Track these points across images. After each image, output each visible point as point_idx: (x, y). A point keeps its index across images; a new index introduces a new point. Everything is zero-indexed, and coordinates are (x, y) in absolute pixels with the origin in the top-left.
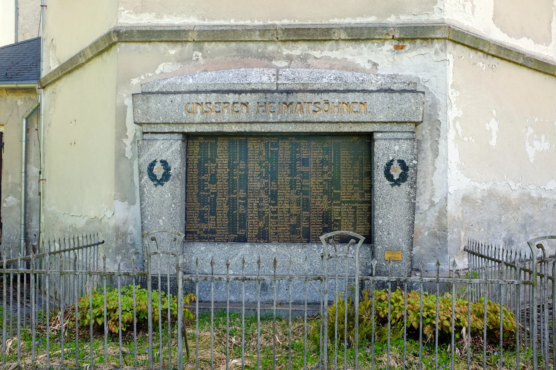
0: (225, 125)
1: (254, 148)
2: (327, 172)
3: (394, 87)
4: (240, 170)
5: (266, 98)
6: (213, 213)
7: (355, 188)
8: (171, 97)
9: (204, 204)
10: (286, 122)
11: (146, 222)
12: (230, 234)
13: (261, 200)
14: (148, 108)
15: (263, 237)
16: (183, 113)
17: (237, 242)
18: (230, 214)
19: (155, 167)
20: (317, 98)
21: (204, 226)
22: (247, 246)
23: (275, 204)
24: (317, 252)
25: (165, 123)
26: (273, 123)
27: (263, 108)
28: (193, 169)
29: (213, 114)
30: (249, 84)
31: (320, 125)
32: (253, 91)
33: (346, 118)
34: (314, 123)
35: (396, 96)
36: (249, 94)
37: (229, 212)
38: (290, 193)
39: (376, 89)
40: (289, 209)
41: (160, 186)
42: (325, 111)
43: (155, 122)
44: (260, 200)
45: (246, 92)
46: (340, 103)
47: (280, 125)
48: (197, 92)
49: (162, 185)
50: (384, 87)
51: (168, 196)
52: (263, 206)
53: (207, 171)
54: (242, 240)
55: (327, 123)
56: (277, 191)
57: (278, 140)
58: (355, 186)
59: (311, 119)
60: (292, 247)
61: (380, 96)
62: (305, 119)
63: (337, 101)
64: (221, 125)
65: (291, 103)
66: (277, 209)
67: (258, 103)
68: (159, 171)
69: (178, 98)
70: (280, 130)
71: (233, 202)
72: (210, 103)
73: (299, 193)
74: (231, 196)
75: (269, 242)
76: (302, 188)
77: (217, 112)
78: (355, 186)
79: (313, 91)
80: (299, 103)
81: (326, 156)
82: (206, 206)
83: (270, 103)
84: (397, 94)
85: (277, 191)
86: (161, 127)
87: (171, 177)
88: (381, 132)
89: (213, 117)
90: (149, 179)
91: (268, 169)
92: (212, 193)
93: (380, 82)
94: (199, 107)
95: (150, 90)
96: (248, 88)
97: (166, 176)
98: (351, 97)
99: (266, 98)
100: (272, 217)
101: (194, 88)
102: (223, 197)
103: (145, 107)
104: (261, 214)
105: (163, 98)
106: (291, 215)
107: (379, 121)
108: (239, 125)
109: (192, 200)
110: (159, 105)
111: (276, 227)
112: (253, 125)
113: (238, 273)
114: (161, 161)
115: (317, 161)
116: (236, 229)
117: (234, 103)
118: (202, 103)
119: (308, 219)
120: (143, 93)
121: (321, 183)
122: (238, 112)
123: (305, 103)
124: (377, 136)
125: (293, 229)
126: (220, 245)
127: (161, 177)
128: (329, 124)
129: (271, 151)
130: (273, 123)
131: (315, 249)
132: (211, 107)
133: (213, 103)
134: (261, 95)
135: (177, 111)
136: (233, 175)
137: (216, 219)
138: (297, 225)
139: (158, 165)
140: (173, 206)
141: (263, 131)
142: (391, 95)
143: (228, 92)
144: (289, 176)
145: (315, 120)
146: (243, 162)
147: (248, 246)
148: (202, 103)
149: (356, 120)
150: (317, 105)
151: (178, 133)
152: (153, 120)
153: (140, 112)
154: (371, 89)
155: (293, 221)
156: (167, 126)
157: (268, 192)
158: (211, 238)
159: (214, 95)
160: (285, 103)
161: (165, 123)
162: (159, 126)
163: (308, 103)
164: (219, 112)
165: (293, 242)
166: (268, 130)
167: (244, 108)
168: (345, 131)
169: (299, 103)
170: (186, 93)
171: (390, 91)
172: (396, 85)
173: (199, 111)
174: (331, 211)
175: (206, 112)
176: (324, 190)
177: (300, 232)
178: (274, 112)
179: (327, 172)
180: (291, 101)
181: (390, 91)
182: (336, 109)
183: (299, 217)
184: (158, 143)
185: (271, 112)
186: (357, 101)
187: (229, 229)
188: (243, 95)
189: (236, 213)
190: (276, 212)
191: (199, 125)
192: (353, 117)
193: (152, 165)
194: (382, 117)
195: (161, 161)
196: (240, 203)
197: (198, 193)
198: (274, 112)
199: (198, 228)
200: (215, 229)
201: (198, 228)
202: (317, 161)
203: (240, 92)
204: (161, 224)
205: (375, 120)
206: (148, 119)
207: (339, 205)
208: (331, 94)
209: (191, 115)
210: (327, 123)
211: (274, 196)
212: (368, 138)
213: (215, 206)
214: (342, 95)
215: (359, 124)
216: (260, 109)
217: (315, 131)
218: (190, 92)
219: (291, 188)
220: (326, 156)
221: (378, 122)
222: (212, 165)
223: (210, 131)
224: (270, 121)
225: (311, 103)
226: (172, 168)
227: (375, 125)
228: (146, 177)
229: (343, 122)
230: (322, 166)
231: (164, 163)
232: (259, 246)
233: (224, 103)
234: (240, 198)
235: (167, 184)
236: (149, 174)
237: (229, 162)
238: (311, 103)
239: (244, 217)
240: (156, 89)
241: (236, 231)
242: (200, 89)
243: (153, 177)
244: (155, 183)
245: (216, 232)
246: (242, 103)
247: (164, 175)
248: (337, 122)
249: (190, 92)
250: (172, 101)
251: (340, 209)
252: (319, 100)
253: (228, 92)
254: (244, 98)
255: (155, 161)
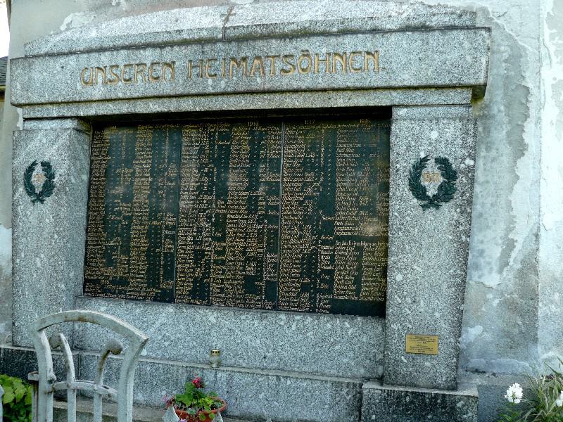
0: (139, 102)
1: (191, 141)
2: (311, 183)
3: (434, 22)
4: (169, 179)
5: (203, 52)
6: (126, 251)
7: (362, 213)
8: (62, 60)
9: (112, 235)
10: (235, 93)
11: (18, 261)
12: (148, 287)
13: (200, 230)
14: (30, 79)
15: (200, 295)
16: (78, 84)
17: (160, 301)
18: (151, 254)
19: (34, 173)
20: (289, 47)
21: (110, 272)
22: (170, 309)
23: (223, 239)
24: (285, 328)
25: (52, 103)
26: (214, 95)
27: (198, 70)
28: (99, 177)
29: (120, 83)
30: (179, 32)
31: (294, 96)
32: (185, 43)
33: (340, 81)
34: (282, 92)
35: (433, 38)
36: (176, 48)
37: (149, 250)
38: (247, 219)
39: (398, 26)
40: (245, 248)
41: (38, 204)
42: (303, 70)
43: (39, 101)
44: (197, 232)
45: (171, 44)
46: (329, 54)
47: (225, 98)
48: (101, 50)
49: (42, 201)
50: (413, 23)
51: (49, 220)
52: (201, 242)
53: (120, 181)
54: (165, 298)
55: (305, 91)
56: (225, 215)
57: (230, 128)
58: (361, 208)
59: (276, 85)
60: (243, 317)
61: (404, 40)
62: (267, 86)
63: (324, 50)
64: (132, 102)
65: (244, 59)
66: (224, 247)
67: (191, 61)
68: (38, 179)
69: (72, 60)
70: (225, 107)
71: (156, 234)
72: (117, 66)
73: (263, 219)
74: (155, 223)
75: (209, 304)
76: (267, 212)
77: (125, 80)
78: (361, 208)
79: (284, 36)
80: (258, 58)
81: (312, 155)
82: (115, 239)
83: (210, 60)
84: (437, 33)
85: (225, 215)
86: (48, 109)
87: (55, 189)
88: (407, 106)
89: (121, 90)
90: (25, 192)
91: (212, 177)
92: (125, 218)
93: (405, 15)
94: (100, 74)
95: (36, 53)
96: (177, 38)
97: (48, 188)
98: (349, 43)
99: (203, 52)
100: (216, 262)
101: (96, 45)
102: (140, 225)
103: (27, 78)
104: (199, 255)
105: (51, 62)
106: (248, 260)
107: (400, 84)
108: (161, 101)
109: (96, 228)
110: (45, 74)
111: (222, 280)
112: (181, 100)
113: (154, 355)
114: (43, 164)
115: (296, 164)
116: (159, 279)
117: (153, 64)
118: (105, 67)
119: (276, 266)
120: (26, 57)
121: (301, 203)
122: (157, 78)
123: (268, 57)
124: (399, 113)
125: (250, 284)
126: (128, 306)
127: (41, 190)
128: (309, 94)
129: (219, 146)
130: (214, 95)
131: (282, 323)
132: (118, 73)
133: (122, 67)
134: (195, 47)
135: (69, 82)
136: (158, 188)
137: (128, 261)
138: (258, 277)
139: (39, 169)
140: (56, 237)
141: (198, 109)
142: (425, 36)
143: (145, 46)
144: (247, 189)
145: (285, 87)
146: (174, 166)
147: (172, 310)
148: (105, 67)
149: (358, 85)
150: (289, 60)
151: (71, 117)
152: (35, 99)
153: (19, 87)
154: (388, 27)
155: (251, 270)
156: (55, 107)
157: (210, 218)
158: (120, 293)
159: (123, 52)
160: (233, 59)
161: (52, 103)
162: (45, 107)
163: (274, 57)
164: (130, 80)
165: (247, 307)
166: (206, 108)
167: (167, 72)
168: (339, 105)
169: (258, 58)
170: (82, 52)
171: (424, 28)
172: (436, 18)
173: (100, 81)
174: (316, 254)
175: (110, 81)
176: (305, 215)
177: (261, 290)
178: (216, 75)
179: (311, 183)
180: (243, 55)
181: (424, 28)
182: (322, 66)
183: (260, 262)
184: (40, 134)
185: (210, 76)
186: (359, 49)
187: (148, 278)
188: (168, 49)
189: (160, 253)
190: (222, 253)
191: (100, 104)
192: (352, 80)
193: (31, 169)
194: (407, 76)
195: (43, 164)
196: (166, 236)
197: (105, 216)
198: (216, 75)
199: (102, 275)
200: (127, 278)
201: (102, 275)
202: (296, 164)
203: (161, 46)
204: (39, 265)
205: (393, 83)
206: (28, 98)
207: (332, 243)
208: (314, 39)
209: (89, 88)
210: (305, 91)
211: (220, 224)
212: (382, 116)
213: (129, 239)
214: (333, 40)
215: (365, 92)
216: (193, 70)
217: (285, 106)
218: (89, 51)
219: (250, 212)
220: (312, 155)
221: (400, 88)
222: (127, 170)
223: (117, 112)
224: (207, 91)
225: (279, 56)
226: (57, 176)
227: (394, 93)
228: (21, 189)
229: (334, 90)
230: (304, 172)
231: (47, 166)
232: (189, 311)
233: (138, 65)
234: (167, 228)
235: (49, 200)
236: (25, 185)
237: (152, 167)
238: (279, 56)
239: (170, 257)
240: (44, 50)
241: (159, 283)
242: (105, 45)
243: (30, 189)
244: (33, 199)
245: (128, 283)
246: (166, 64)
247: (45, 186)
248: (324, 90)
249: (89, 51)
250: (62, 67)
251: (334, 251)
252: (293, 51)
253: (145, 46)
254: (168, 55)
255: (34, 164)
